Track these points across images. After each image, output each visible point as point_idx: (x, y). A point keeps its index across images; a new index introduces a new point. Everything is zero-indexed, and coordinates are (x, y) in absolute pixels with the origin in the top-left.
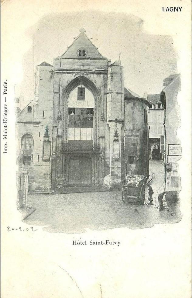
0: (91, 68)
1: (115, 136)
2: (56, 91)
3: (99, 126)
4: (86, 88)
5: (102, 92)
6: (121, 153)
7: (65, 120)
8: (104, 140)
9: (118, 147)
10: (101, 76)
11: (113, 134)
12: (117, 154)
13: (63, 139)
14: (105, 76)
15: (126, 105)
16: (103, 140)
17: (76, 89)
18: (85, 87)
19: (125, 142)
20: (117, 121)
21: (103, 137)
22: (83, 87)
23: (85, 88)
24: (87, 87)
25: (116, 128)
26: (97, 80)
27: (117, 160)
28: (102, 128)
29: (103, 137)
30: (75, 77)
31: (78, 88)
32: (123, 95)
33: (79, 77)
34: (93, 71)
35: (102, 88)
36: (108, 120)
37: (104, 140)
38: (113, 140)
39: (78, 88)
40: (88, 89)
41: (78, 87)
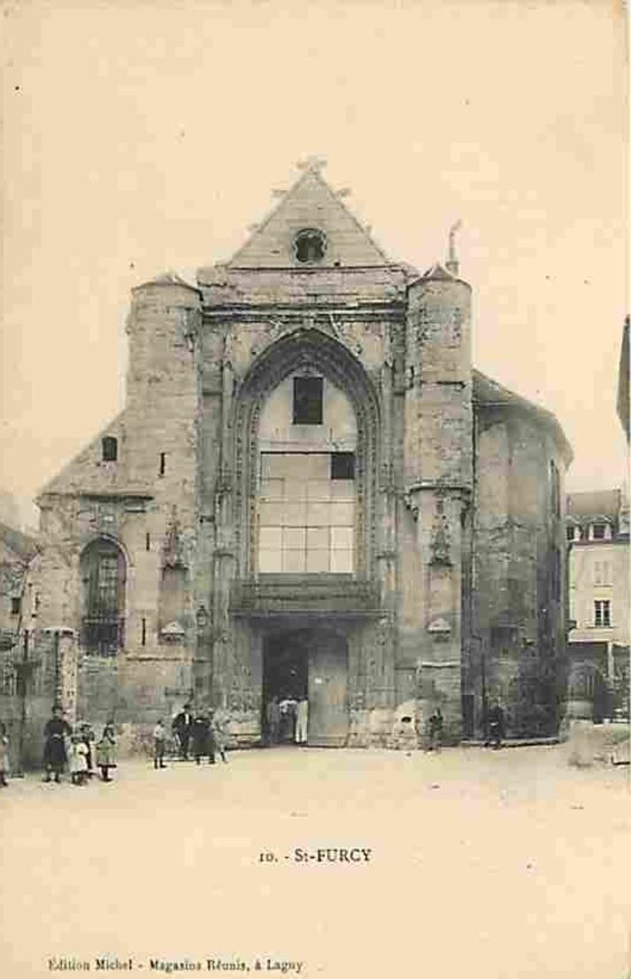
1: (434, 547)
2: (210, 387)
3: (373, 516)
4: (325, 380)
5: (386, 391)
8: (393, 568)
9: (446, 589)
10: (380, 330)
11: (425, 539)
12: (444, 616)
13: (238, 565)
15: (479, 432)
16: (389, 565)
18: (320, 375)
19: (475, 575)
20: (439, 490)
21: (390, 556)
23: (321, 379)
24: (327, 375)
25: (441, 516)
26: (371, 348)
27: (441, 637)
28: (386, 522)
29: (390, 556)
30: (283, 334)
31: (296, 379)
37: (393, 568)
39: (296, 379)
40: (333, 381)
41: (295, 374)
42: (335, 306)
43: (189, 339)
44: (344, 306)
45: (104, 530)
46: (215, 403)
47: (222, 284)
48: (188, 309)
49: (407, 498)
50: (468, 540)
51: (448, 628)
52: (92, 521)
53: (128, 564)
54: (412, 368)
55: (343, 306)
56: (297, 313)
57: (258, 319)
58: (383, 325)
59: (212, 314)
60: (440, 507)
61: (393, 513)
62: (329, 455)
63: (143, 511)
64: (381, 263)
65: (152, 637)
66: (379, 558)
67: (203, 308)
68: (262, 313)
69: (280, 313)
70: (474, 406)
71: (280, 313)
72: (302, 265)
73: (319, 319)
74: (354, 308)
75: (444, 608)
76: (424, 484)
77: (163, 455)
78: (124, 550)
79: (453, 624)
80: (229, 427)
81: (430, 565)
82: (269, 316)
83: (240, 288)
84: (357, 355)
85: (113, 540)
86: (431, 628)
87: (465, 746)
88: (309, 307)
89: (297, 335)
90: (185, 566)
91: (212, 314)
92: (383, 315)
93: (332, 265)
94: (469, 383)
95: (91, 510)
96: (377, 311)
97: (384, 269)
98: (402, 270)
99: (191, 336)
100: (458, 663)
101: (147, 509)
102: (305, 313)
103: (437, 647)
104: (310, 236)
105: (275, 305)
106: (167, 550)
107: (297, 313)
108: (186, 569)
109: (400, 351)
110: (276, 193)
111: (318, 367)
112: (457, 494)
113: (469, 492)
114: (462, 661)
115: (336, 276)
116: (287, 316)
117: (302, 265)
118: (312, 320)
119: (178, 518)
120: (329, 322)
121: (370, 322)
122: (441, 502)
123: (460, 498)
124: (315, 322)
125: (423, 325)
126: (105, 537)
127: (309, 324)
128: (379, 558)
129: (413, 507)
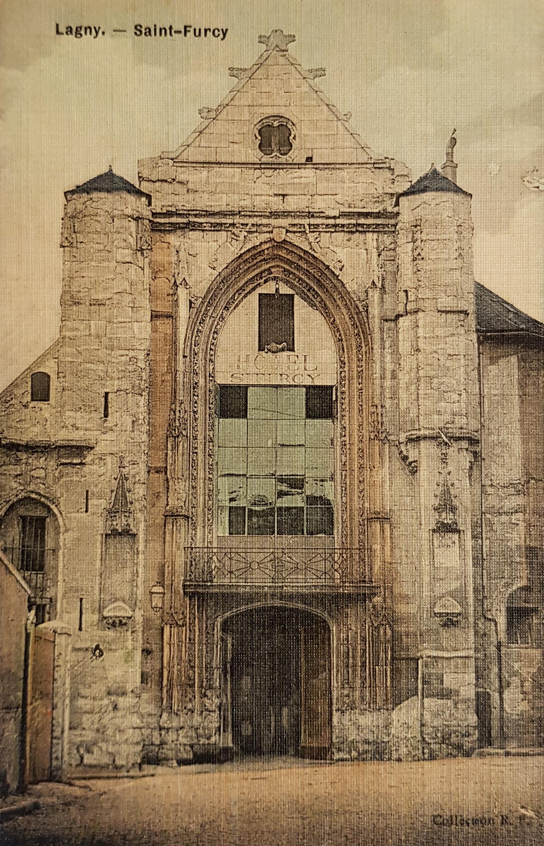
0: (320, 204)
5: (375, 311)
6: (471, 589)
7: (200, 437)
12: (451, 594)
14: (387, 240)
16: (383, 530)
17: (254, 298)
22: (285, 290)
30: (249, 246)
31: (260, 295)
32: (472, 321)
33: (264, 247)
34: (328, 218)
35: (375, 295)
36: (403, 437)
38: (433, 526)
39: (260, 295)
41: (259, 290)
42: (311, 215)
43: (139, 253)
44: (322, 215)
45: (32, 487)
46: (164, 326)
47: (169, 180)
48: (137, 219)
49: (403, 448)
50: (477, 498)
51: (458, 609)
52: (17, 476)
53: (62, 530)
54: (406, 291)
55: (320, 214)
56: (265, 221)
57: (217, 227)
58: (369, 235)
59: (162, 221)
60: (444, 459)
61: (387, 464)
62: (304, 389)
63: (81, 464)
64: (364, 159)
65: (91, 618)
66: (370, 520)
67: (154, 215)
68: (223, 221)
69: (245, 221)
70: (478, 338)
71: (245, 221)
72: (266, 159)
73: (291, 229)
74: (334, 218)
75: (455, 585)
76: (422, 432)
77: (107, 394)
78: (56, 511)
79: (463, 601)
80: (185, 357)
81: (434, 531)
82: (233, 225)
83: (190, 186)
84: (337, 272)
85: (43, 499)
86: (437, 610)
87: (481, 755)
88: (275, 215)
89: (264, 247)
90: (135, 531)
91: (162, 221)
92: (369, 226)
93: (303, 161)
94: (471, 309)
95: (18, 461)
96: (362, 221)
97: (368, 166)
98: (389, 168)
99: (142, 250)
100: (472, 653)
101: (88, 460)
102: (273, 222)
103: (444, 633)
104: (276, 124)
105: (240, 212)
106: (112, 513)
107: (265, 221)
108: (134, 535)
109: (390, 267)
110: (233, 72)
111: (287, 282)
112: (464, 444)
113: (478, 442)
114: (476, 650)
115: (308, 173)
116: (253, 225)
117: (266, 159)
118: (284, 231)
119: (125, 471)
120: (305, 231)
121: (352, 232)
122: (445, 455)
123: (467, 449)
124: (287, 231)
125: (418, 243)
126: (33, 496)
127: (280, 235)
128: (370, 520)
129: (410, 460)
